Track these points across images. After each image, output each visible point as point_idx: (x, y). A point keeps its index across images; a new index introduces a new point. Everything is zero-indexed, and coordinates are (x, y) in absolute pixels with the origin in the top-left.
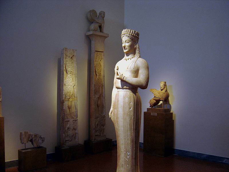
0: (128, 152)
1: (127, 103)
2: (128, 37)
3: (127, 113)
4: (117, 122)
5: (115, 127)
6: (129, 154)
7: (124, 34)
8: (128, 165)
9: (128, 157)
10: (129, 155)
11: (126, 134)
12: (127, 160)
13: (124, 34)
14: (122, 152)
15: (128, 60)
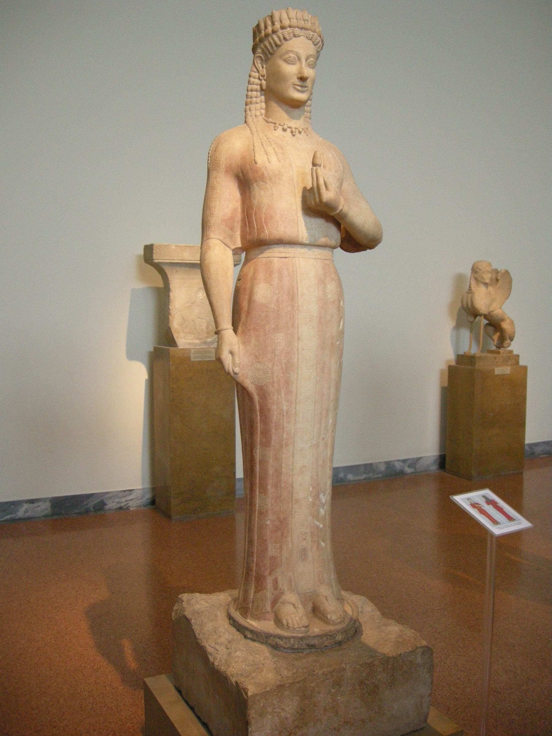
0: (321, 496)
1: (334, 302)
2: (315, 45)
3: (332, 344)
4: (288, 383)
5: (275, 407)
6: (324, 501)
7: (302, 28)
8: (323, 544)
9: (322, 512)
10: (326, 501)
11: (323, 425)
12: (318, 527)
13: (302, 28)
14: (297, 501)
15: (300, 132)
